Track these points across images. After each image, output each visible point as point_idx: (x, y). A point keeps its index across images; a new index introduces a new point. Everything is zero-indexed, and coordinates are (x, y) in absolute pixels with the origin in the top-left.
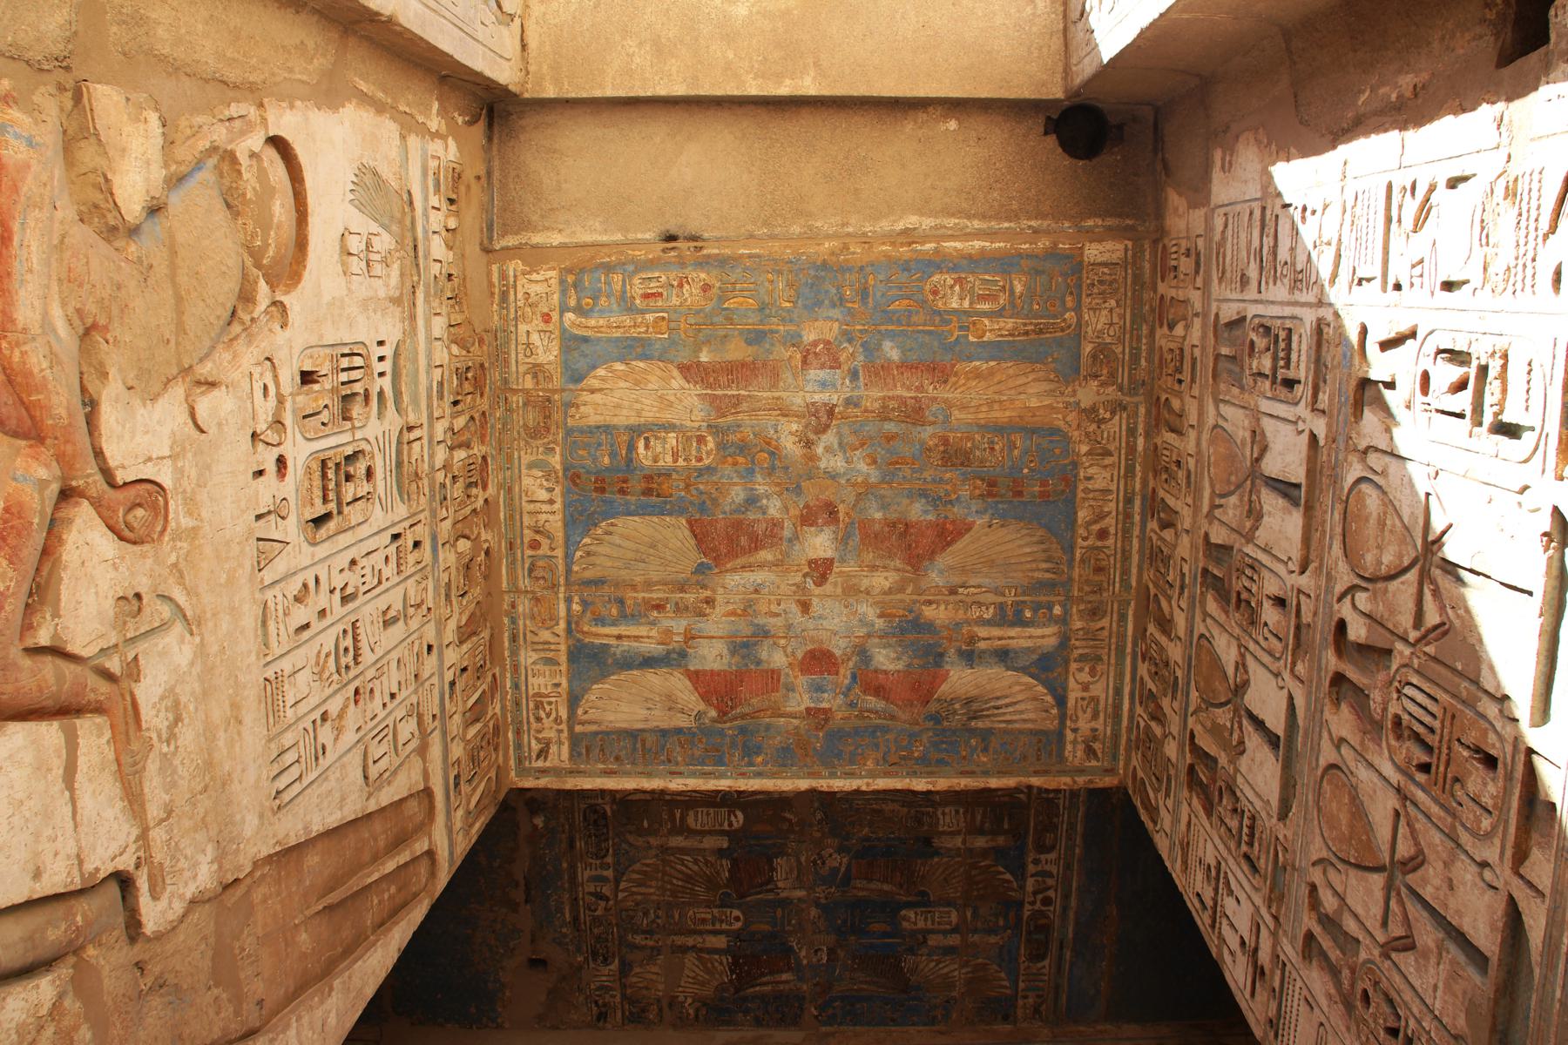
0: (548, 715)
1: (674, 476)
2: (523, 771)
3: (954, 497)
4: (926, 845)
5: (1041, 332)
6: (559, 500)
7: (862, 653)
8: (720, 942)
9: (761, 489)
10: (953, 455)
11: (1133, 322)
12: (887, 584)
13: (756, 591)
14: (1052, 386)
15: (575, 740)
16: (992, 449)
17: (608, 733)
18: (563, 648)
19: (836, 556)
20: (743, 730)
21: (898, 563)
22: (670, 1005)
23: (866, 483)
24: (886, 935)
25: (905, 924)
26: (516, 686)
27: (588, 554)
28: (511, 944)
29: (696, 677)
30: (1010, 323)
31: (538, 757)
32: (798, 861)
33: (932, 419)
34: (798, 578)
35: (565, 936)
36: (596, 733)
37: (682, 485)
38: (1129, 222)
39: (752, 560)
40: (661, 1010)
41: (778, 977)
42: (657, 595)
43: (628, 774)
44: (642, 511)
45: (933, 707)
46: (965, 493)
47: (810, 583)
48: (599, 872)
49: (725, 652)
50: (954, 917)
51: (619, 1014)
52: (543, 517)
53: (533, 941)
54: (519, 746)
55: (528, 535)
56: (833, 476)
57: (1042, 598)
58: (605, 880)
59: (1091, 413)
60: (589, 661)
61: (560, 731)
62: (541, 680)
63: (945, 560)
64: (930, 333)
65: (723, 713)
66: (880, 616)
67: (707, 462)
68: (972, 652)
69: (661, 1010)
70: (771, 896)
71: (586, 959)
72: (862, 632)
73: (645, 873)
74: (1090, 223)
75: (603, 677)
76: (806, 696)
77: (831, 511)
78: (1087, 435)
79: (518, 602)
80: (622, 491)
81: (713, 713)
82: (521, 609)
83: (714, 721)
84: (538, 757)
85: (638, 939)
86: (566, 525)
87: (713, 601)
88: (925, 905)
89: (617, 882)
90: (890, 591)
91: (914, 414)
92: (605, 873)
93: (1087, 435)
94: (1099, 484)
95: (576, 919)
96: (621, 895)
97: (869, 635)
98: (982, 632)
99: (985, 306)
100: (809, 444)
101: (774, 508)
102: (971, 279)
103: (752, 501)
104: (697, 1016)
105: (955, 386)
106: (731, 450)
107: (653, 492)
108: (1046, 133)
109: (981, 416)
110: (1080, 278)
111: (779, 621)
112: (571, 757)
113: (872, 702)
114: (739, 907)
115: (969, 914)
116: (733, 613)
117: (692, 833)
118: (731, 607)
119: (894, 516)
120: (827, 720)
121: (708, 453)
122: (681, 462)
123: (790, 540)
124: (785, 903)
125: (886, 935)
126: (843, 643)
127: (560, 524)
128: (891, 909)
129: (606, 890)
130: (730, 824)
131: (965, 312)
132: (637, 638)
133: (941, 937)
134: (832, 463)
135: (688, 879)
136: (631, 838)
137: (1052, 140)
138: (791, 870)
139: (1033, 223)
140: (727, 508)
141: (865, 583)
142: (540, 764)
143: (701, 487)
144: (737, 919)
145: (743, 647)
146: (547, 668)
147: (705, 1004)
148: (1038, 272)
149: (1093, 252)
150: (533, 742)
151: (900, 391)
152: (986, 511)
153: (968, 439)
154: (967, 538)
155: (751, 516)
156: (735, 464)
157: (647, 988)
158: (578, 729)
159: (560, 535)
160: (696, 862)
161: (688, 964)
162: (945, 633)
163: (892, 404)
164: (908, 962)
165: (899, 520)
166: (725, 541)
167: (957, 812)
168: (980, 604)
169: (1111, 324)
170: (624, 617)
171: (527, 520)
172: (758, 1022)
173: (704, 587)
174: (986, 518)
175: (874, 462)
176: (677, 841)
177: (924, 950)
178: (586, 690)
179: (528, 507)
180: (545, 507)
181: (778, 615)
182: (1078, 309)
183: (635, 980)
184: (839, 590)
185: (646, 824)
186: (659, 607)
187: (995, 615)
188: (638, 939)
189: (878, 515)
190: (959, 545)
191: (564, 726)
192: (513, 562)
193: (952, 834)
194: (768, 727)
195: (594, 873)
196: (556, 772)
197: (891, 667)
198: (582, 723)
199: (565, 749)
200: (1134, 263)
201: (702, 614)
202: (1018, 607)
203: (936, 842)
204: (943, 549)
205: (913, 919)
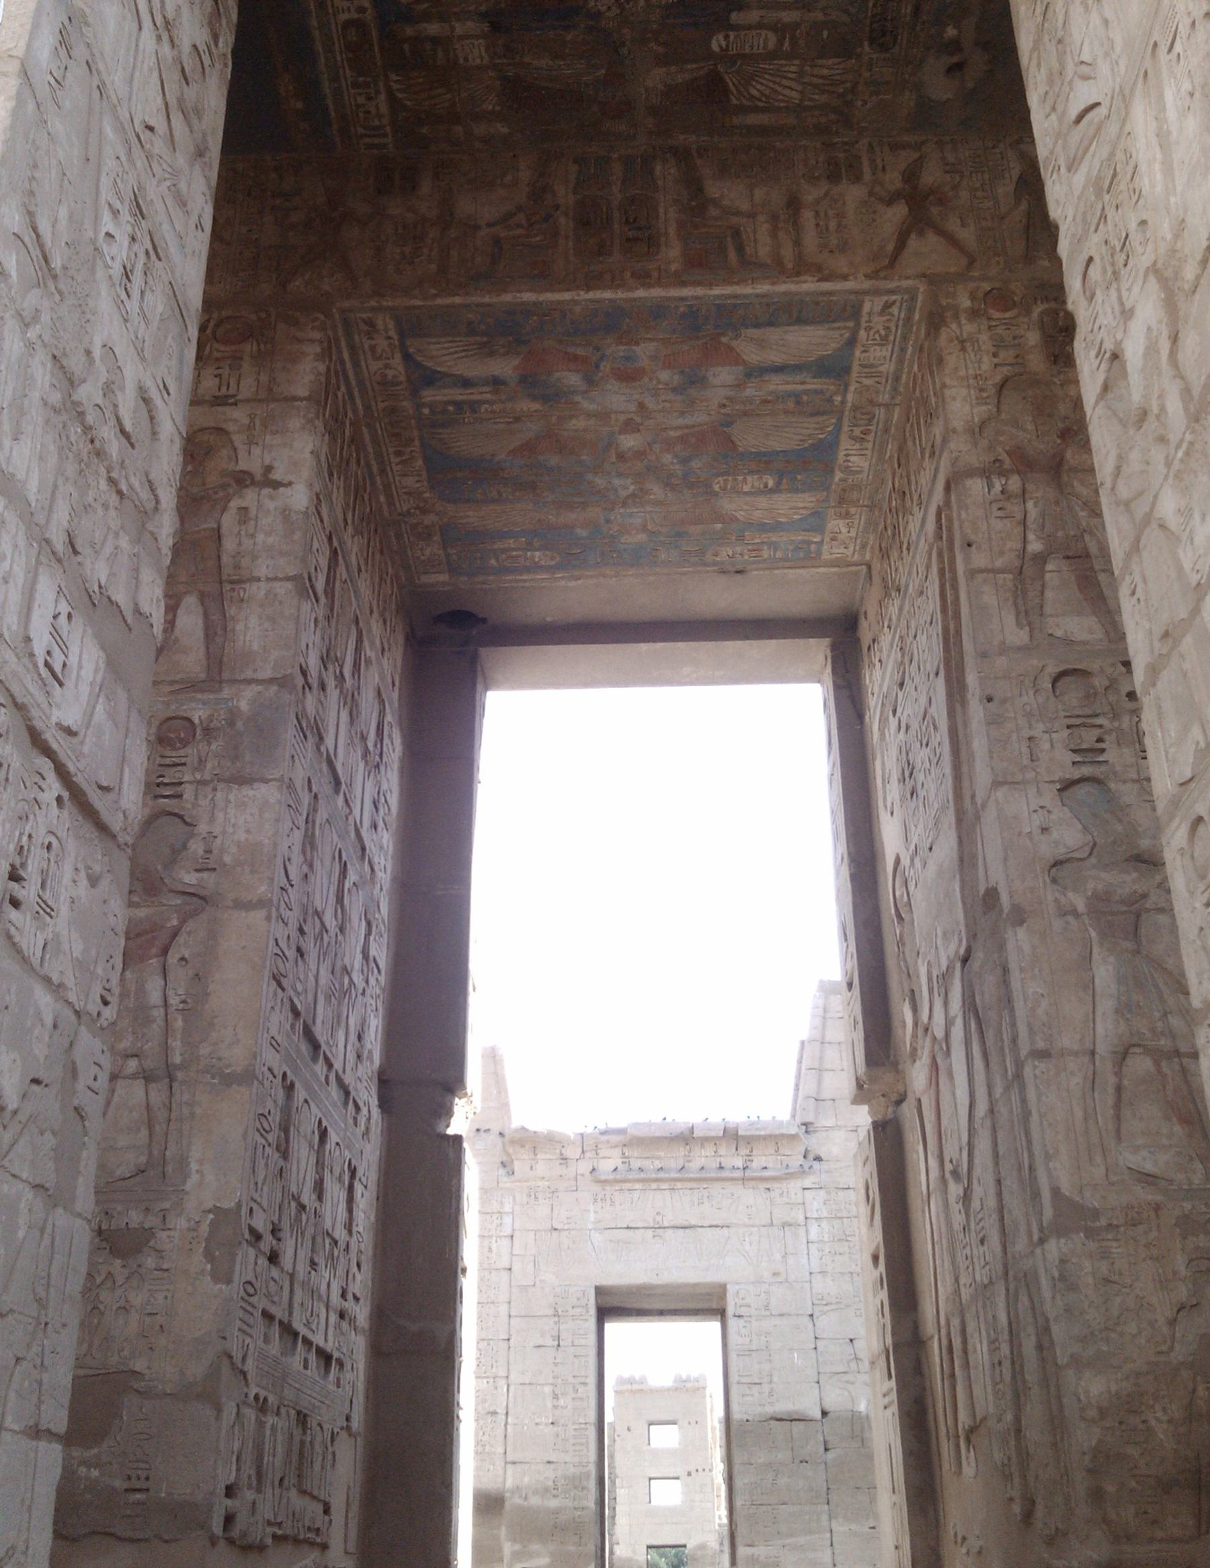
4: (496, 23)
7: (591, 382)
9: (677, 467)
12: (574, 421)
18: (854, 375)
23: (596, 473)
27: (821, 429)
29: (737, 360)
30: (495, 547)
31: (894, 302)
36: (834, 321)
43: (808, 293)
55: (870, 437)
59: (424, 511)
60: (834, 368)
61: (869, 321)
62: (878, 354)
83: (723, 334)
90: (571, 417)
97: (586, 392)
98: (488, 396)
101: (667, 458)
111: (664, 397)
112: (863, 302)
113: (580, 351)
116: (702, 401)
117: (775, 27)
122: (740, 478)
130: (727, 37)
136: (845, 18)
137: (481, 616)
141: (592, 422)
142: (894, 298)
145: (694, 380)
149: (444, 577)
158: (851, 324)
159: (844, 438)
167: (466, 59)
171: (870, 445)
174: (497, 459)
176: (788, 17)
182: (448, 555)
184: (613, 416)
185: (825, 34)
186: (766, 402)
191: (864, 325)
192: (886, 421)
193: (468, 37)
196: (877, 292)
198: (845, 328)
203: (486, 27)
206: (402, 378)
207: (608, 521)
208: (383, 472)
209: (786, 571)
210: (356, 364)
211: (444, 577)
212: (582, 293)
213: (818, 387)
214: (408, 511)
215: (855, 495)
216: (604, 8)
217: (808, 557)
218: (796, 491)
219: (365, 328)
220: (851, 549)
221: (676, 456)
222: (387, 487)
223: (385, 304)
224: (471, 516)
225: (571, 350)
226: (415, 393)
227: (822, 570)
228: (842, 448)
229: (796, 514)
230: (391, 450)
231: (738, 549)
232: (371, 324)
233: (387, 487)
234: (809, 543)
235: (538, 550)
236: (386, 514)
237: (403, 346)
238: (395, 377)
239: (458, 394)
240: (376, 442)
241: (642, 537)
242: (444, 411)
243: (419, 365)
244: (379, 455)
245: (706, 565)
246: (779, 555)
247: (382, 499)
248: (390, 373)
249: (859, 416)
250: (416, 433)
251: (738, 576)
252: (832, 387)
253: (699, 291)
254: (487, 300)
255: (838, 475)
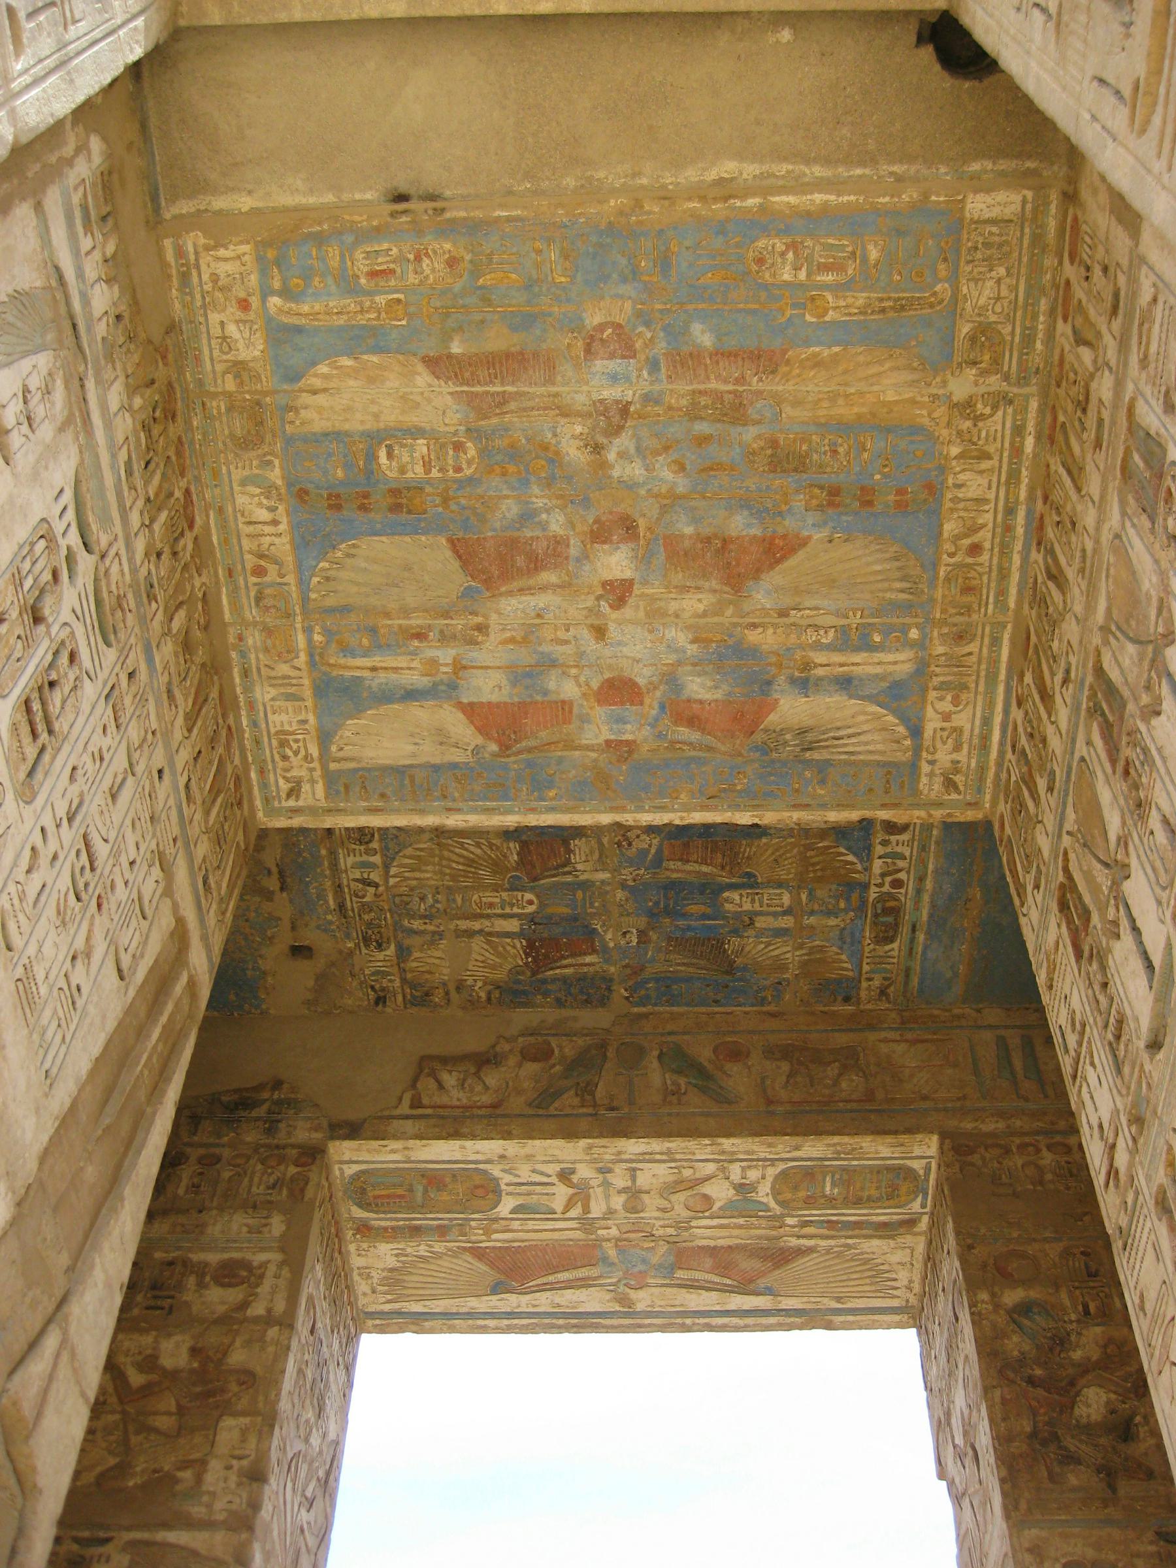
0: (296, 753)
1: (428, 489)
2: (271, 812)
3: (784, 508)
5: (903, 308)
6: (284, 520)
7: (671, 679)
8: (513, 926)
10: (783, 459)
11: (1028, 295)
12: (701, 607)
13: (539, 616)
14: (915, 376)
15: (330, 779)
16: (835, 452)
17: (369, 770)
18: (306, 682)
19: (637, 576)
20: (530, 764)
21: (714, 584)
22: (458, 989)
24: (705, 917)
25: (728, 906)
26: (255, 724)
27: (328, 579)
28: (269, 933)
29: (470, 710)
31: (289, 796)
32: (600, 843)
33: (756, 416)
34: (590, 602)
35: (331, 923)
36: (355, 770)
37: (438, 500)
38: (1030, 164)
39: (531, 582)
40: (447, 993)
41: (580, 960)
42: (417, 621)
43: (397, 811)
44: (392, 530)
45: (759, 737)
46: (799, 502)
47: (604, 606)
48: (365, 858)
49: (505, 682)
50: (786, 899)
51: (400, 998)
52: (267, 540)
53: (293, 928)
54: (264, 785)
55: (250, 561)
56: (630, 486)
57: (895, 620)
58: (373, 866)
59: (966, 407)
60: (339, 695)
61: (311, 770)
62: (284, 717)
63: (775, 578)
64: (753, 312)
65: (505, 748)
66: (693, 642)
67: (468, 472)
68: (807, 680)
69: (447, 993)
70: (569, 879)
71: (357, 945)
72: (671, 659)
73: (418, 858)
74: (975, 167)
75: (358, 712)
76: (604, 728)
77: (629, 528)
78: (959, 433)
79: (246, 633)
80: (363, 508)
81: (494, 747)
82: (250, 641)
83: (494, 755)
84: (289, 796)
85: (417, 924)
86: (295, 547)
87: (487, 627)
88: (751, 887)
89: (387, 867)
90: (705, 614)
91: (734, 411)
92: (372, 859)
93: (959, 433)
94: (972, 492)
95: (341, 907)
96: (392, 881)
97: (679, 663)
98: (820, 658)
99: (829, 278)
100: (597, 449)
101: (556, 524)
102: (809, 243)
103: (528, 516)
104: (489, 999)
105: (786, 377)
106: (499, 458)
107: (403, 506)
108: (920, 41)
109: (821, 413)
110: (959, 240)
111: (569, 649)
113: (684, 733)
114: (532, 890)
115: (804, 897)
116: (512, 640)
118: (508, 634)
119: (707, 531)
120: (630, 752)
121: (469, 463)
123: (578, 560)
124: (585, 885)
125: (705, 917)
126: (647, 672)
127: (288, 547)
128: (711, 891)
129: (375, 876)
131: (801, 285)
132: (396, 669)
133: (770, 919)
134: (628, 471)
135: (470, 862)
137: (927, 53)
138: (592, 852)
139: (895, 168)
140: (498, 525)
141: (673, 606)
142: (291, 803)
143: (463, 502)
144: (531, 902)
146: (289, 704)
147: (498, 987)
148: (900, 232)
149: (978, 205)
150: (281, 782)
151: (714, 385)
152: (825, 523)
153: (803, 440)
154: (801, 554)
155: (529, 534)
156: (504, 474)
157: (430, 972)
158: (333, 766)
159: (289, 559)
160: (478, 845)
161: (475, 947)
162: (774, 659)
163: (703, 401)
164: (733, 944)
165: (716, 536)
166: (496, 562)
168: (816, 628)
169: (998, 299)
170: (378, 646)
171: (246, 544)
172: (560, 1003)
173: (474, 613)
175: (682, 468)
177: (751, 932)
178: (339, 726)
179: (250, 529)
180: (268, 529)
181: (566, 642)
182: (954, 279)
183: (415, 964)
184: (641, 614)
186: (420, 636)
187: (836, 638)
188: (417, 924)
189: (689, 530)
190: (792, 562)
191: (316, 765)
194: (560, 760)
195: (358, 859)
196: (313, 811)
197: (708, 696)
198: (338, 760)
199: (320, 789)
200: (1034, 219)
201: (473, 642)
202: (865, 631)
204: (771, 567)
205: (736, 901)
206: (932, 695)
207: (654, 366)
208: (1010, 511)
209: (312, 200)
210: (987, 722)
211: (978, 205)
212: (677, 822)
213: (351, 662)
214: (995, 408)
215: (239, 425)
216: (643, 837)
217: (284, 242)
218: (337, 435)
219: (959, 779)
220: (205, 277)
221: (544, 526)
222: (1014, 477)
223: (923, 814)
224: (890, 386)
225: (695, 736)
226: (922, 669)
227: (245, 203)
228: (285, 539)
229: (326, 377)
230: (985, 557)
231: (412, 279)
232: (950, 784)
233: (1014, 477)
234: (286, 293)
235: (788, 284)
236: (1034, 405)
237: (917, 750)
238: (941, 699)
239: (863, 664)
240: (1004, 575)
241: (593, 318)
242: (887, 631)
243: (904, 719)
244: (1005, 550)
245: (474, 228)
246: (333, 253)
247: (1029, 443)
248: (946, 706)
249: (282, 605)
250: (939, 594)
251: (404, 188)
252: (332, 661)
253: (533, 820)
254: (796, 815)
255: (276, 475)
